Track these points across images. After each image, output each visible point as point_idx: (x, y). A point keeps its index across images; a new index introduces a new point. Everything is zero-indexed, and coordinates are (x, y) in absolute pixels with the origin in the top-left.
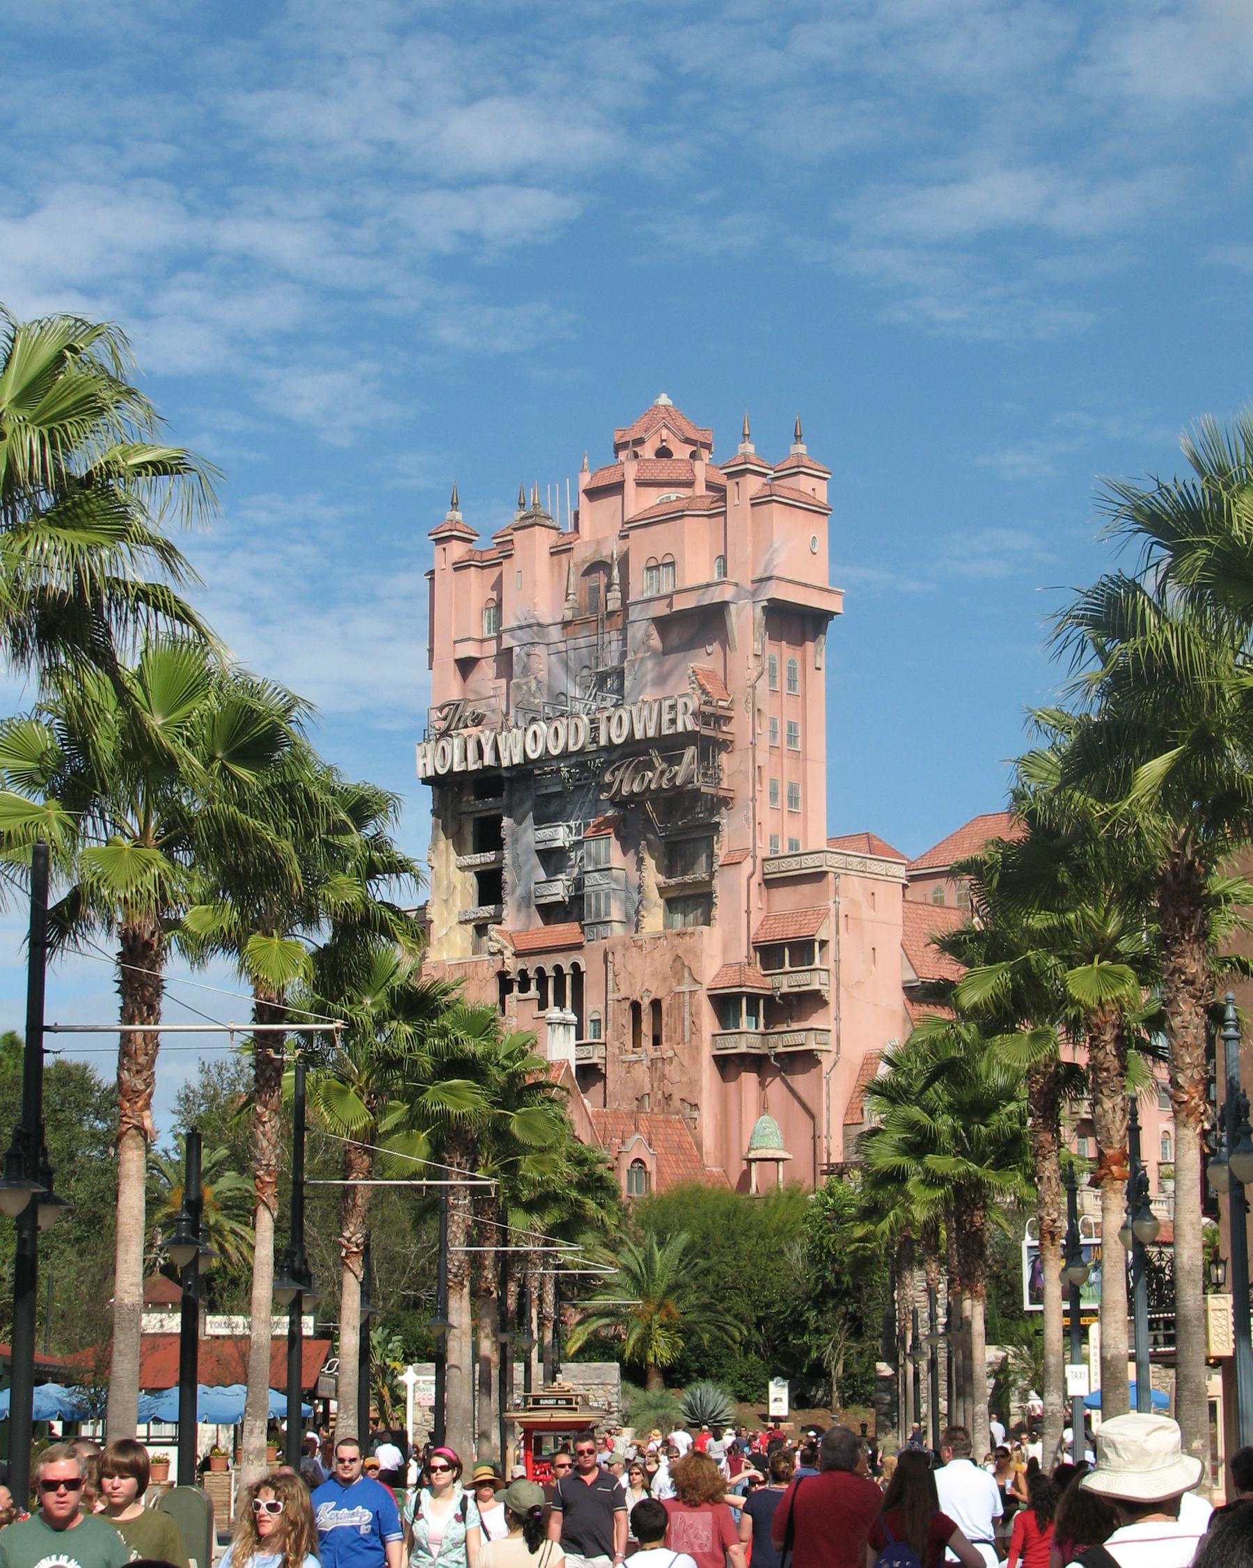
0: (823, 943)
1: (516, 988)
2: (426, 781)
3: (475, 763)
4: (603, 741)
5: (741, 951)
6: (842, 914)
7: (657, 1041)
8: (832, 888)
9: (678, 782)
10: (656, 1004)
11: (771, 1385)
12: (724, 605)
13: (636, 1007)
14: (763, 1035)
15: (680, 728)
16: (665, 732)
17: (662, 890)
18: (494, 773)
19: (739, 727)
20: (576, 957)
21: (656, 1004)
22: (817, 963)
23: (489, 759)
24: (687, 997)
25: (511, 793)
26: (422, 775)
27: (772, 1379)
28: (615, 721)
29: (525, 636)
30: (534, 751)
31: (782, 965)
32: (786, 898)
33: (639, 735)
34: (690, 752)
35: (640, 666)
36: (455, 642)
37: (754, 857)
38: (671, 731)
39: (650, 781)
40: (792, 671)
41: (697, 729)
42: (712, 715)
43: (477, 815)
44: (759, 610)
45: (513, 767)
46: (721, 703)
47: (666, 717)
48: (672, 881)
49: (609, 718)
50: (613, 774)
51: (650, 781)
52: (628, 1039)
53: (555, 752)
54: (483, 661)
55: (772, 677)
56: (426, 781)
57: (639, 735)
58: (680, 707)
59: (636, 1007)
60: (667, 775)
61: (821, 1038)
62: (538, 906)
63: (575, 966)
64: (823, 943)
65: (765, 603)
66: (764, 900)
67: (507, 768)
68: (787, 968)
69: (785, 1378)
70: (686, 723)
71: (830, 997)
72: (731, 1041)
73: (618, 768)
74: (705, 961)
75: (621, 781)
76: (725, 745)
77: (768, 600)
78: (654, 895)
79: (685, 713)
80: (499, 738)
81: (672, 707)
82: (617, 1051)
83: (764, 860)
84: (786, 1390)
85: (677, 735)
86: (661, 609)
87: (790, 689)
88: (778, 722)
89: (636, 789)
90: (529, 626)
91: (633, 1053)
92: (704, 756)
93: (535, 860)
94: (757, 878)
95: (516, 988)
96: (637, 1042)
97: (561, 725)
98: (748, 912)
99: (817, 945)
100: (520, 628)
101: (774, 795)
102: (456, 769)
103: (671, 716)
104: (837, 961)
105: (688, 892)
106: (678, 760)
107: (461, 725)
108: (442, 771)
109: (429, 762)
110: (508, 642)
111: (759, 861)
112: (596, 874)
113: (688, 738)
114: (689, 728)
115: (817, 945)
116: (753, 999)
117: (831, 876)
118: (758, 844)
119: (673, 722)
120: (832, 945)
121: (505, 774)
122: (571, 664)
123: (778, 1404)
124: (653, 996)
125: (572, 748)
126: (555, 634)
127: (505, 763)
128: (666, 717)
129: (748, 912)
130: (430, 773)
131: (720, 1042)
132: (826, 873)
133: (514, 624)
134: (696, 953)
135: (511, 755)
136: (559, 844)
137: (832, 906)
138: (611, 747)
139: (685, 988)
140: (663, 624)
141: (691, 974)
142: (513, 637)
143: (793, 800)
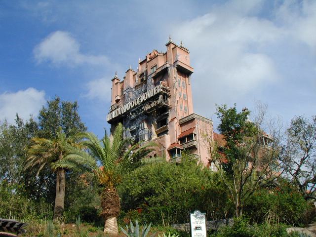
2: (109, 122)
5: (176, 140)
8: (196, 123)
11: (192, 216)
12: (167, 68)
15: (158, 92)
23: (120, 113)
25: (125, 121)
27: (193, 212)
28: (144, 96)
29: (127, 91)
31: (185, 141)
32: (185, 128)
34: (161, 96)
40: (183, 84)
45: (124, 113)
55: (179, 84)
64: (195, 135)
69: (202, 211)
71: (198, 147)
74: (166, 142)
76: (169, 97)
78: (155, 133)
84: (204, 221)
86: (153, 75)
92: (164, 98)
93: (130, 133)
94: (178, 124)
101: (181, 108)
109: (109, 118)
113: (160, 93)
117: (196, 120)
119: (157, 91)
120: (197, 135)
121: (123, 116)
123: (198, 232)
126: (134, 90)
134: (164, 141)
139: (162, 150)
140: (155, 78)
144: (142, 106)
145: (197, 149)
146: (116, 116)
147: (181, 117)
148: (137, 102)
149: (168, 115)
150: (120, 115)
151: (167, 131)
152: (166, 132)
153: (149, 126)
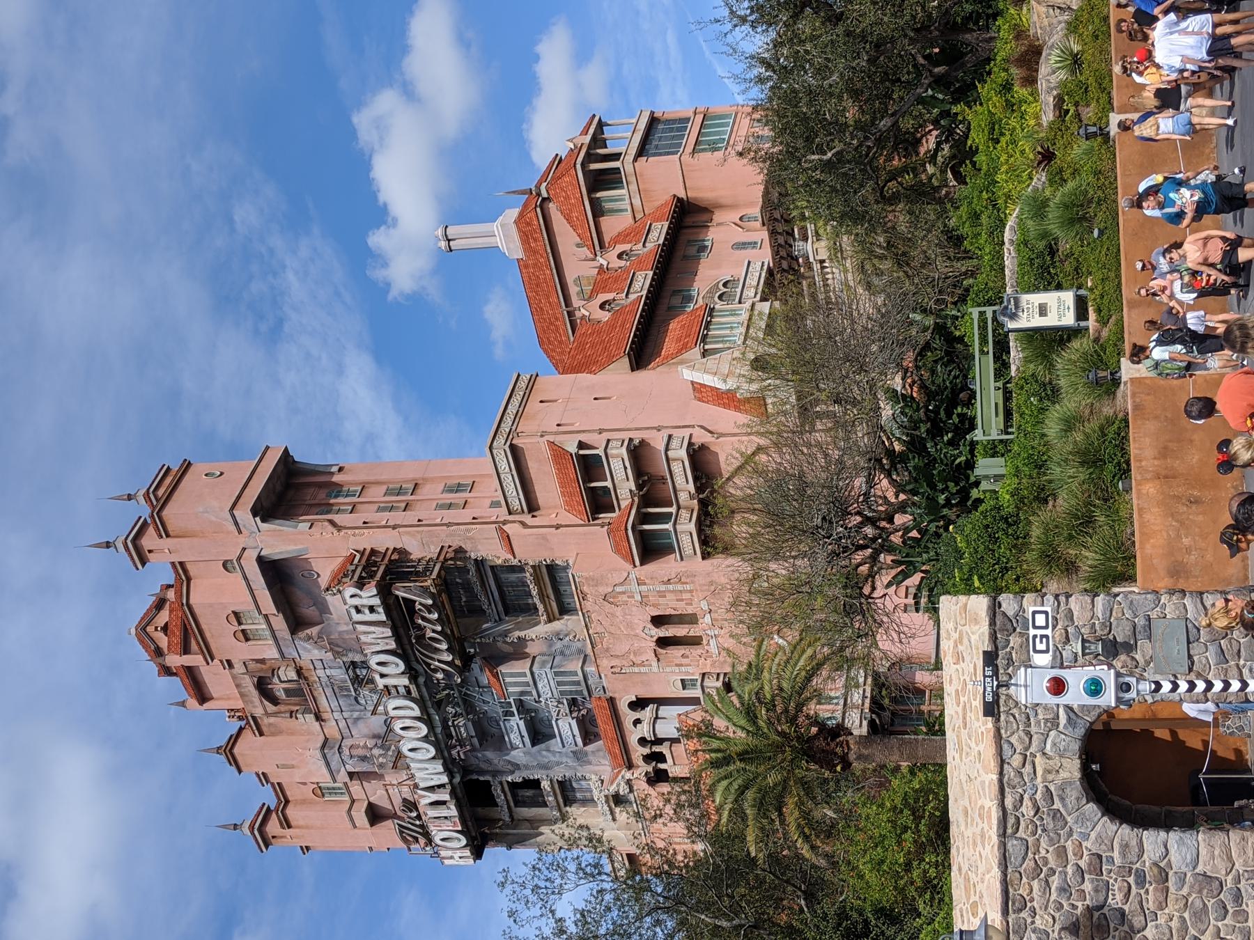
0: (582, 445)
1: (662, 766)
2: (478, 854)
3: (449, 808)
4: (405, 681)
6: (556, 429)
7: (691, 619)
9: (430, 602)
13: (663, 642)
14: (679, 508)
15: (376, 601)
16: (383, 617)
17: (550, 621)
18: (458, 790)
19: (384, 541)
20: (623, 706)
21: (658, 621)
22: (600, 452)
23: (446, 797)
24: (644, 588)
26: (471, 861)
29: (335, 760)
30: (428, 751)
31: (605, 488)
33: (392, 645)
34: (401, 591)
35: (338, 646)
36: (355, 827)
37: (505, 522)
38: (381, 610)
39: (434, 631)
41: (374, 583)
42: (363, 569)
43: (512, 804)
44: (264, 526)
46: (356, 561)
47: (368, 617)
48: (541, 607)
49: (382, 676)
50: (435, 670)
51: (434, 631)
52: (695, 651)
53: (424, 730)
54: (371, 799)
56: (478, 854)
58: (356, 601)
59: (663, 642)
60: (427, 615)
61: (675, 443)
62: (585, 744)
64: (582, 445)
65: (258, 519)
66: (550, 512)
67: (451, 776)
68: (608, 484)
70: (370, 595)
72: (685, 541)
73: (429, 665)
75: (440, 661)
77: (255, 515)
78: (557, 625)
79: (360, 597)
80: (422, 785)
81: (358, 611)
82: (709, 662)
83: (510, 513)
85: (385, 604)
87: (355, 495)
88: (382, 505)
89: (444, 646)
90: (325, 756)
91: (708, 644)
92: (405, 577)
94: (527, 519)
95: (662, 766)
97: (397, 726)
98: (558, 527)
99: (582, 452)
100: (328, 764)
102: (460, 828)
103: (367, 611)
104: (601, 431)
105: (550, 591)
106: (410, 603)
107: (418, 823)
109: (456, 852)
110: (343, 777)
111: (511, 518)
112: (540, 686)
113: (385, 592)
114: (374, 592)
115: (582, 452)
116: (644, 518)
118: (493, 519)
119: (372, 609)
120: (584, 438)
121: (457, 779)
122: (356, 714)
124: (650, 626)
125: (417, 712)
127: (444, 779)
128: (368, 617)
129: (558, 527)
130: (467, 853)
131: (688, 550)
132: (513, 448)
133: (325, 770)
137: (547, 438)
138: (411, 672)
141: (621, 584)
142: (339, 771)
143: (458, 488)
144: (429, 682)
145: (642, 442)
146: (453, 811)
147: (495, 504)
148: (403, 711)
149: (480, 563)
150: (453, 793)
151: (552, 569)
152: (552, 574)
153: (518, 652)
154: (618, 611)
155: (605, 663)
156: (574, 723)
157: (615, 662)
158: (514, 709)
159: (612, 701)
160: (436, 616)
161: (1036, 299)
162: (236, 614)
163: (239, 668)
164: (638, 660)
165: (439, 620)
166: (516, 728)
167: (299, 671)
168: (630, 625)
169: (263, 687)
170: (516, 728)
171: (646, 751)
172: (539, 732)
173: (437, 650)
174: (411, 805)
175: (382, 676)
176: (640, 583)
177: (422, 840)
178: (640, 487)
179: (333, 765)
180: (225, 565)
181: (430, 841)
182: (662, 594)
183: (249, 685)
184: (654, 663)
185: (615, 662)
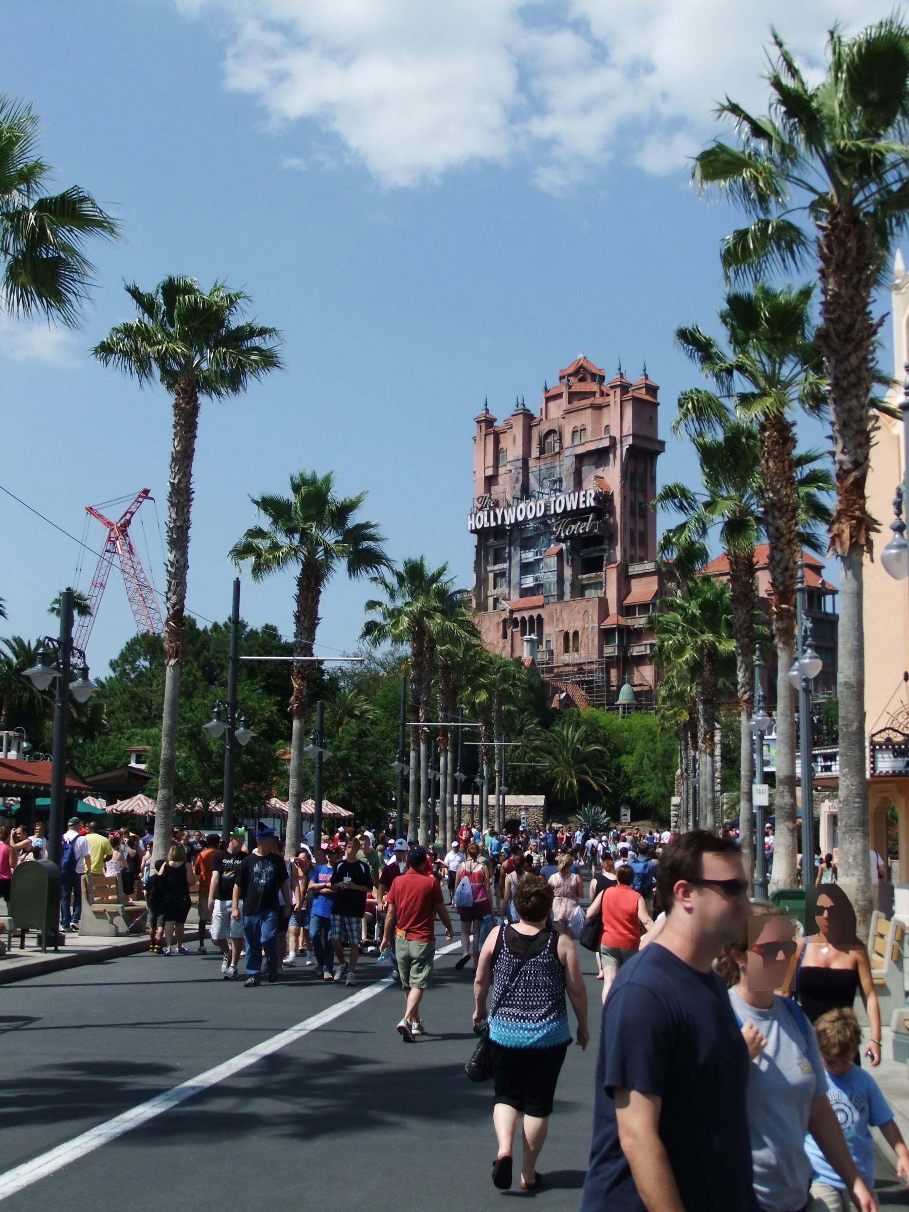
2: (472, 532)
7: (577, 650)
10: (576, 634)
13: (567, 635)
15: (588, 505)
16: (582, 506)
21: (576, 634)
33: (569, 508)
45: (511, 524)
47: (582, 499)
49: (555, 502)
52: (562, 649)
53: (530, 516)
56: (472, 532)
57: (569, 508)
58: (588, 495)
59: (567, 635)
63: (539, 616)
68: (637, 616)
70: (591, 502)
80: (505, 511)
81: (584, 496)
85: (586, 508)
86: (581, 450)
96: (567, 650)
97: (532, 504)
100: (515, 461)
108: (479, 527)
109: (472, 523)
114: (593, 504)
119: (585, 502)
125: (539, 515)
127: (508, 523)
130: (473, 528)
135: (510, 519)
136: (532, 560)
140: (580, 459)
146: (493, 524)
154: (581, 616)
155: (558, 607)
156: (532, 585)
157: (558, 611)
158: (539, 557)
159: (542, 606)
160: (581, 531)
161: (629, 814)
162: (584, 429)
163: (562, 422)
164: (560, 622)
165: (579, 533)
166: (529, 556)
167: (559, 453)
168: (574, 621)
169: (551, 432)
170: (529, 556)
171: (519, 619)
172: (526, 568)
173: (564, 532)
174: (497, 504)
175: (555, 502)
176: (593, 628)
177: (479, 506)
178: (636, 629)
179: (515, 463)
180: (607, 426)
181: (481, 509)
182: (588, 637)
183: (554, 426)
184: (558, 629)
185: (558, 611)
